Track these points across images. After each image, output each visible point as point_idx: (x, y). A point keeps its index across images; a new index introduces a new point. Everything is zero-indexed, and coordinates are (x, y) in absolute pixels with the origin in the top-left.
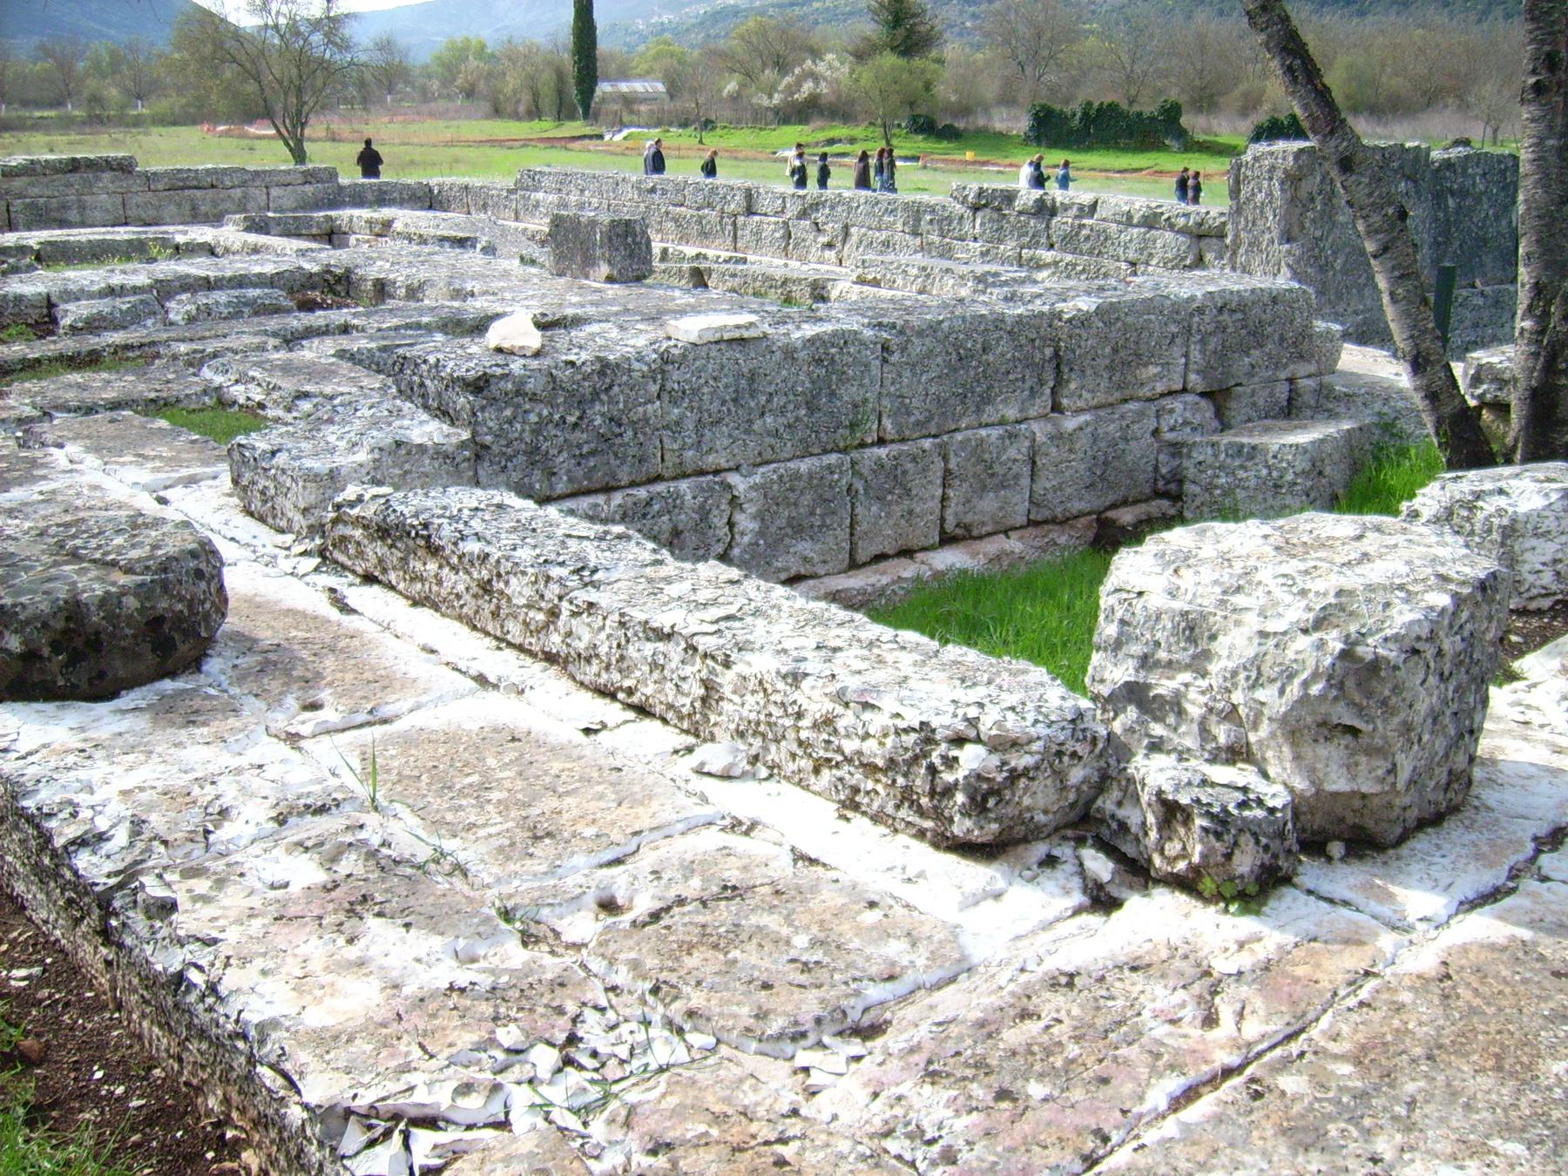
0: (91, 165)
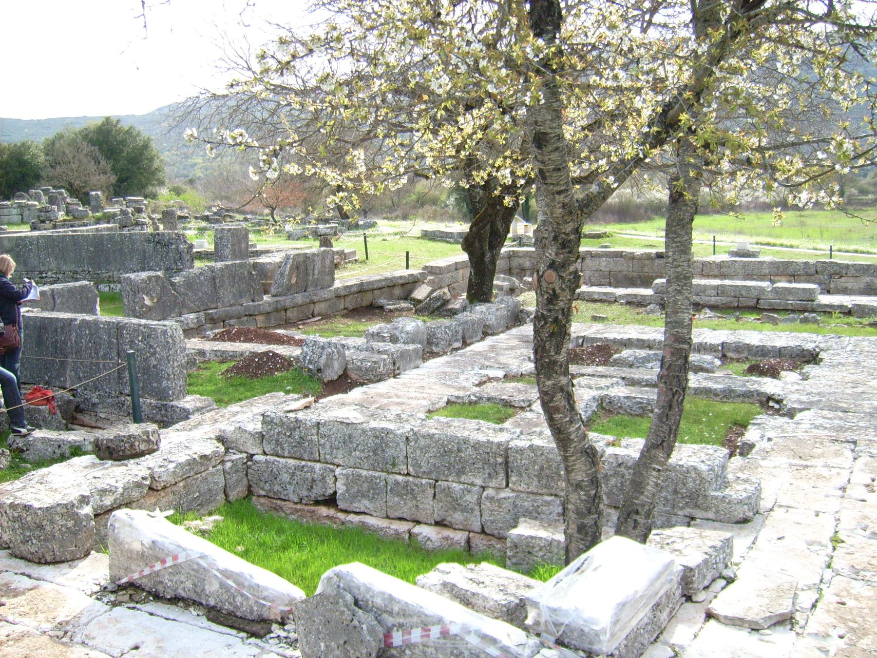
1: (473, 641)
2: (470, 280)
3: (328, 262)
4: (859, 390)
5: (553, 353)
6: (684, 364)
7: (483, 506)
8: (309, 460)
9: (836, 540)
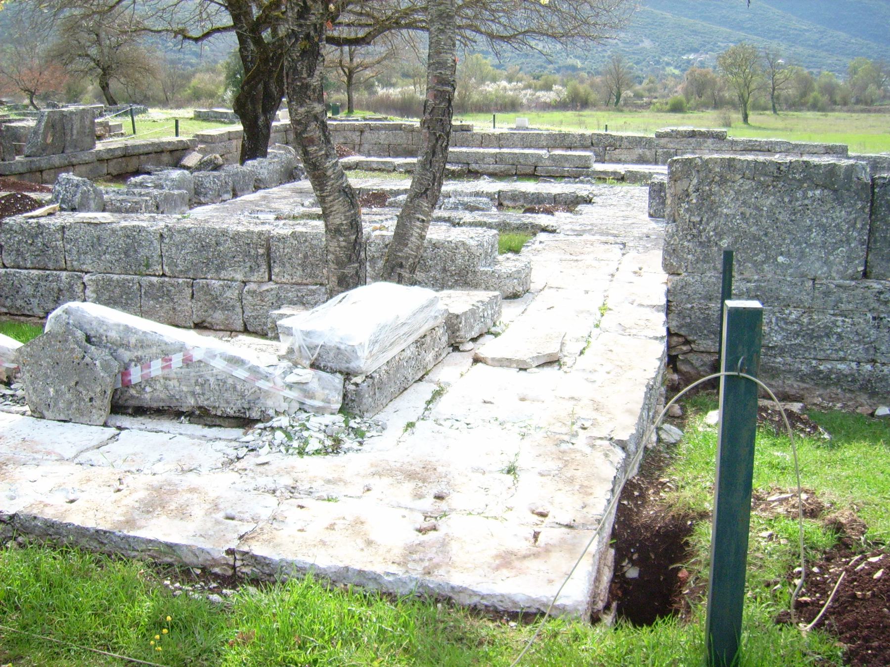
0: (702, 134)
1: (219, 365)
2: (243, 145)
3: (87, 123)
4: (630, 221)
5: (305, 75)
6: (448, 108)
7: (244, 302)
8: (55, 270)
9: (604, 309)
